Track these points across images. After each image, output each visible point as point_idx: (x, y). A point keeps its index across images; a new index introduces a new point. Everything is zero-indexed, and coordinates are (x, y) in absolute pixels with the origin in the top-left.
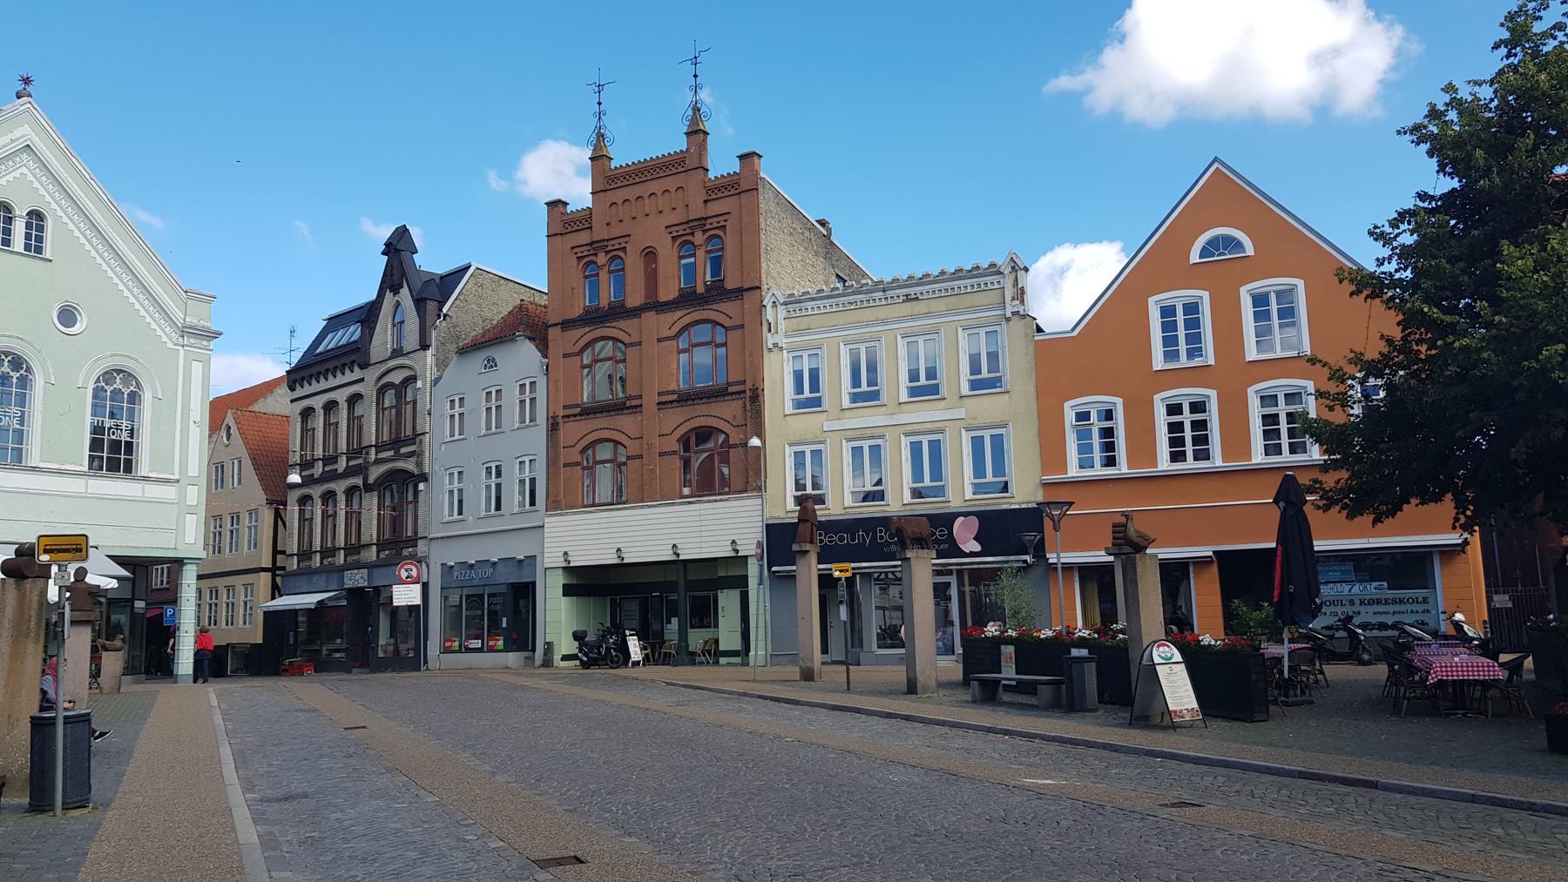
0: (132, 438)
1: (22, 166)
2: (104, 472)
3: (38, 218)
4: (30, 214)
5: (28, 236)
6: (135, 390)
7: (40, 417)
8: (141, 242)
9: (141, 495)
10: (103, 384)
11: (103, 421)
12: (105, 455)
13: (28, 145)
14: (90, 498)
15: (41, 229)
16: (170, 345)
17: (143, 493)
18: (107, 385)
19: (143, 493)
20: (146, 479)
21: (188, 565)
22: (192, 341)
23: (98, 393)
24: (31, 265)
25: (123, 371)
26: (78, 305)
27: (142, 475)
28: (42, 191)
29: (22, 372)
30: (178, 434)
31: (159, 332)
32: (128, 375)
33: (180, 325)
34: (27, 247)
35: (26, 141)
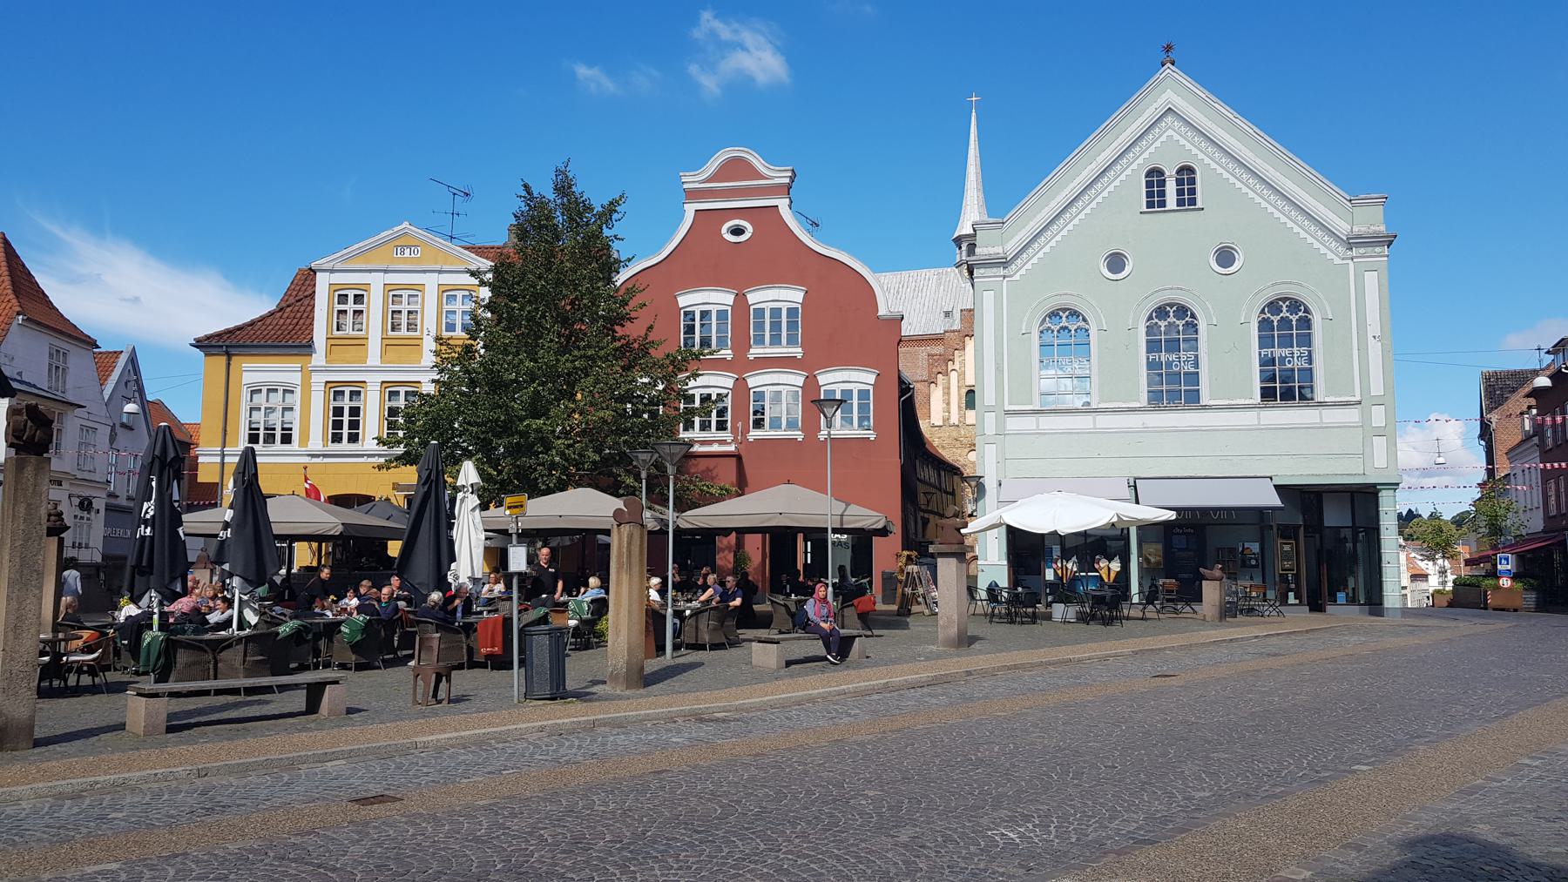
0: (1311, 364)
1: (1167, 129)
2: (1297, 401)
3: (1189, 172)
4: (1180, 171)
5: (1180, 192)
6: (1304, 315)
7: (1206, 359)
8: (1294, 163)
9: (1035, 428)
10: (1269, 315)
11: (1272, 352)
12: (1278, 385)
13: (1170, 108)
14: (1262, 429)
15: (1192, 181)
16: (1337, 261)
17: (1038, 426)
18: (1282, 317)
19: (1038, 426)
20: (1322, 404)
21: (1383, 491)
22: (1362, 250)
23: (1265, 325)
24: (1188, 218)
25: (1289, 299)
26: (1233, 243)
27: (1319, 400)
28: (1188, 146)
29: (1187, 319)
30: (1355, 352)
31: (1323, 250)
32: (1295, 305)
33: (1345, 238)
34: (1180, 203)
35: (1167, 104)
